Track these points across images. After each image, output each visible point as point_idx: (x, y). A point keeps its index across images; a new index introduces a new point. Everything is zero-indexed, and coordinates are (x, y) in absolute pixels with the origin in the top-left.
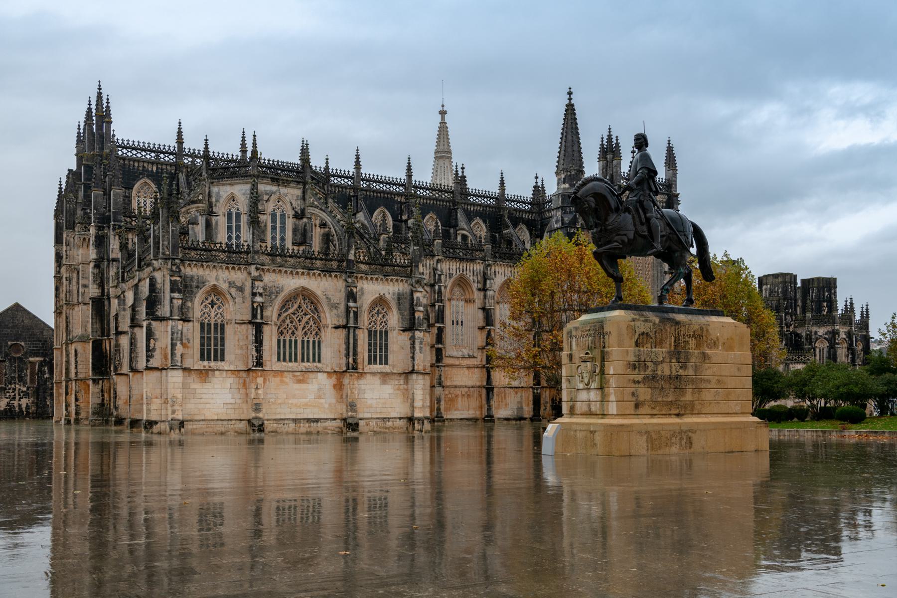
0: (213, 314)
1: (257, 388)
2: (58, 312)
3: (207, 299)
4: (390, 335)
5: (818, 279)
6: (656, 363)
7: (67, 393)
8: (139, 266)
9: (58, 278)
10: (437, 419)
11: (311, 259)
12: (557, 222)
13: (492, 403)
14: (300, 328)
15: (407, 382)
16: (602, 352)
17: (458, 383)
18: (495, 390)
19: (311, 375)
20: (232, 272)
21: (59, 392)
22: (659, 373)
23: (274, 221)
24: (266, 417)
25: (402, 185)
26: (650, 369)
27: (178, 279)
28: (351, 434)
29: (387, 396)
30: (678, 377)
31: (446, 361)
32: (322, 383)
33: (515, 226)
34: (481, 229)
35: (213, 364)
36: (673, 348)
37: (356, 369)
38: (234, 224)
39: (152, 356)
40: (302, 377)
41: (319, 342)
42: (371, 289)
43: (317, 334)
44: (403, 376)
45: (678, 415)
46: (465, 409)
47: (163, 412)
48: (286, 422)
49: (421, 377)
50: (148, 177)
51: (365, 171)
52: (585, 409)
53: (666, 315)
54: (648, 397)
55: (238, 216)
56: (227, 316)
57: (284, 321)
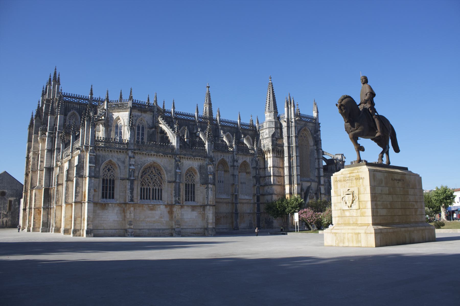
0: (109, 175)
1: (130, 213)
4: (196, 186)
12: (266, 135)
13: (238, 221)
18: (239, 214)
19: (157, 206)
27: (93, 156)
29: (195, 217)
35: (108, 201)
41: (161, 190)
43: (160, 186)
44: (202, 207)
48: (144, 230)
49: (211, 207)
50: (75, 110)
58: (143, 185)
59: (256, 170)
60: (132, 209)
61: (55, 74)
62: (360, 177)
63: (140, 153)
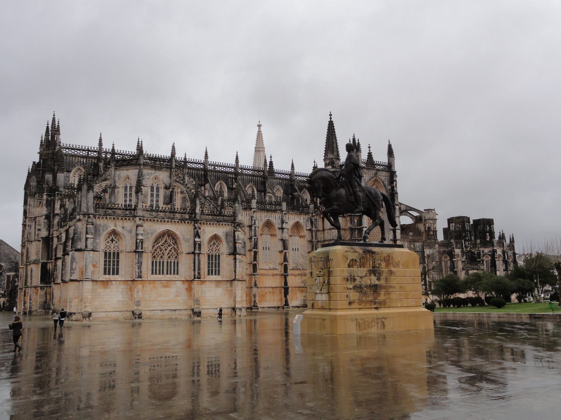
0: (112, 247)
2: (23, 246)
3: (109, 238)
5: (483, 219)
6: (361, 277)
7: (25, 295)
8: (70, 218)
9: (24, 225)
10: (252, 308)
11: (173, 212)
13: (288, 297)
14: (166, 254)
15: (231, 285)
16: (329, 271)
17: (267, 285)
18: (290, 289)
19: (172, 283)
20: (125, 221)
21: (20, 294)
22: (363, 283)
23: (152, 190)
24: (144, 309)
25: (233, 168)
27: (91, 226)
28: (196, 318)
30: (376, 286)
31: (259, 272)
32: (180, 287)
33: (301, 191)
34: (280, 192)
35: (112, 277)
37: (200, 278)
38: (128, 193)
40: (167, 284)
41: (178, 262)
42: (208, 231)
43: (176, 257)
44: (229, 282)
45: (376, 308)
46: (272, 301)
47: (80, 307)
49: (240, 282)
51: (211, 160)
52: (320, 305)
53: (367, 248)
54: (357, 298)
55: (131, 188)
56: (121, 249)
57: (156, 250)
58: (154, 257)
59: (312, 233)
60: (140, 286)
61: (54, 120)
63: (150, 220)
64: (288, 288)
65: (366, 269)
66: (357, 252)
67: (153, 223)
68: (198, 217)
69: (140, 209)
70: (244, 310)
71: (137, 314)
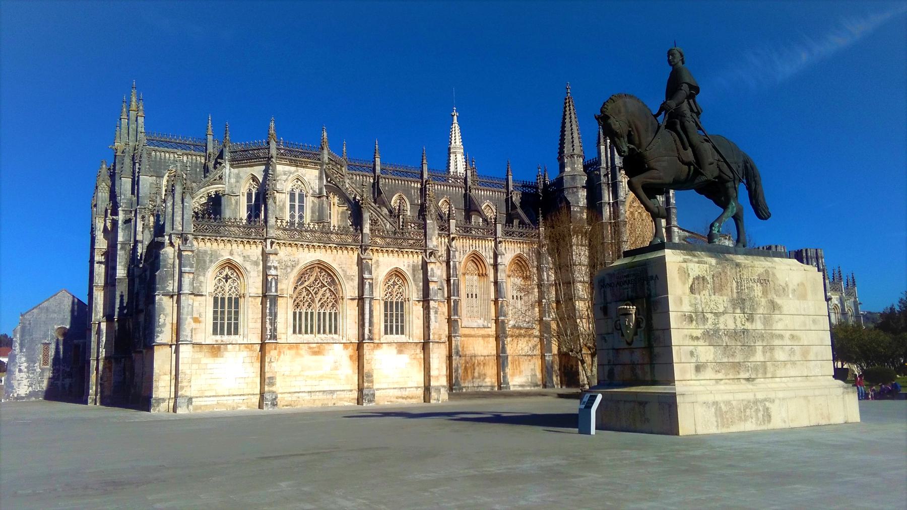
0: (227, 289)
4: (406, 305)
18: (510, 358)
19: (326, 346)
20: (247, 246)
22: (722, 326)
26: (710, 321)
27: (190, 253)
30: (745, 331)
31: (462, 331)
35: (226, 338)
36: (735, 295)
39: (161, 332)
40: (318, 350)
42: (384, 263)
43: (333, 306)
45: (748, 380)
57: (300, 294)
62: (650, 274)
64: (507, 357)
65: (725, 298)
66: (705, 263)
67: (294, 249)
68: (367, 241)
69: (272, 227)
70: (443, 391)
71: (268, 397)
